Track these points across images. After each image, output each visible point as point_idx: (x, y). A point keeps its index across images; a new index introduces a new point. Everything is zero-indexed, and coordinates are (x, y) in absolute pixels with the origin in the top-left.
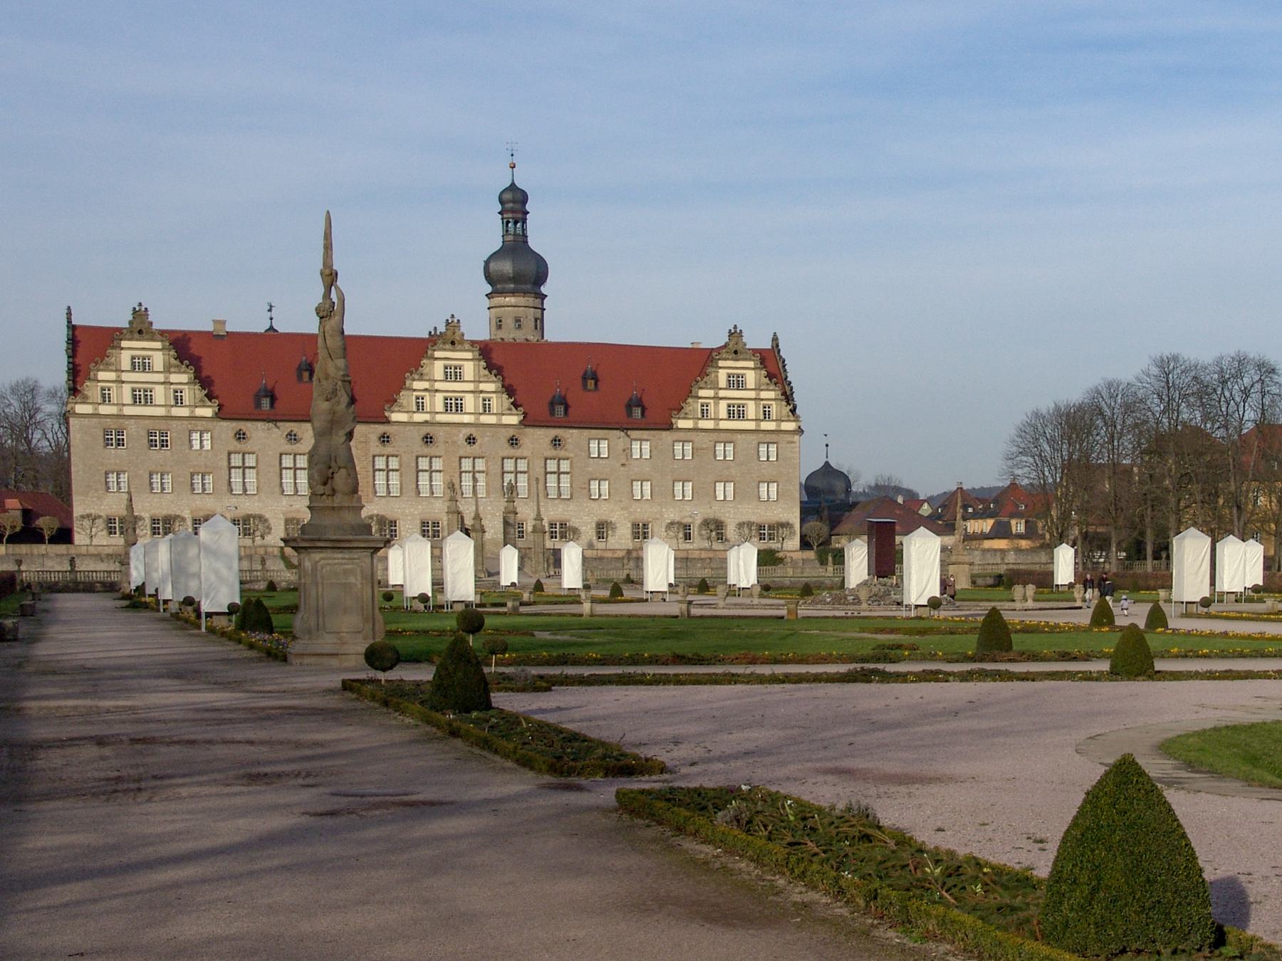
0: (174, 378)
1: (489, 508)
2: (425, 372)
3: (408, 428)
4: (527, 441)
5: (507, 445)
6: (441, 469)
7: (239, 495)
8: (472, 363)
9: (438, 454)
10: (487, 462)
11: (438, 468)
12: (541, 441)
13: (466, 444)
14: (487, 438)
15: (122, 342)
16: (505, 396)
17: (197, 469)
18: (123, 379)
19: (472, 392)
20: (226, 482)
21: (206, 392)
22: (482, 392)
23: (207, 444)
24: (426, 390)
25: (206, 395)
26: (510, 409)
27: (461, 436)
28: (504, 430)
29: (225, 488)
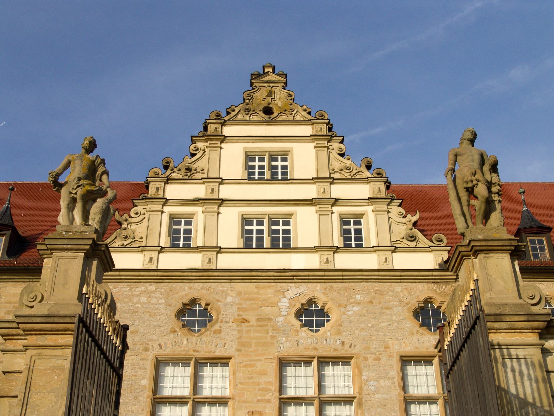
2: (198, 165)
3: (141, 287)
5: (412, 324)
6: (227, 394)
8: (309, 148)
9: (219, 352)
10: (359, 369)
11: (217, 393)
13: (298, 324)
14: (356, 309)
16: (395, 210)
19: (313, 202)
22: (336, 201)
26: (413, 238)
27: (284, 303)
28: (399, 287)
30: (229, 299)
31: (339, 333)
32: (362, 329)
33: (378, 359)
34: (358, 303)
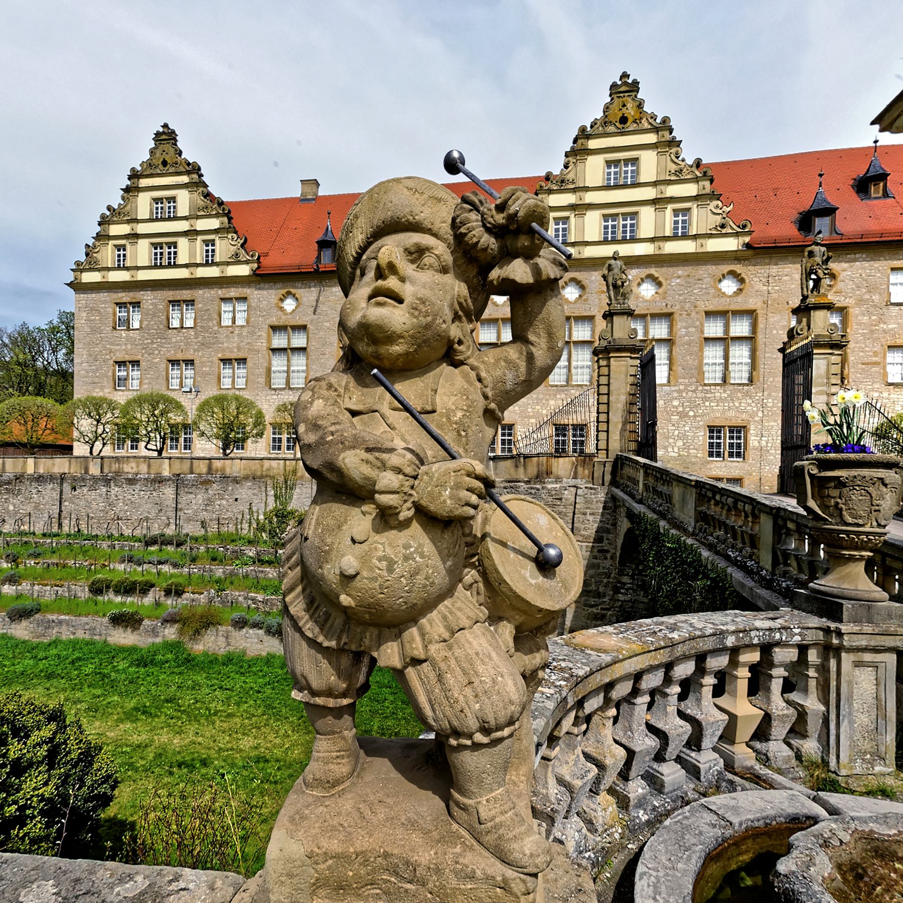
0: (202, 224)
1: (676, 403)
4: (757, 279)
7: (281, 389)
12: (785, 278)
14: (678, 281)
15: (141, 180)
17: (228, 355)
18: (139, 232)
19: (654, 202)
20: (263, 371)
21: (242, 241)
22: (672, 200)
23: (240, 321)
24: (573, 207)
25: (242, 246)
29: (262, 380)
30: (593, 278)
31: (664, 298)
32: (680, 295)
33: (689, 315)
34: (679, 277)
